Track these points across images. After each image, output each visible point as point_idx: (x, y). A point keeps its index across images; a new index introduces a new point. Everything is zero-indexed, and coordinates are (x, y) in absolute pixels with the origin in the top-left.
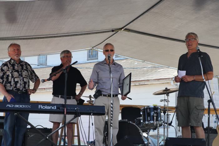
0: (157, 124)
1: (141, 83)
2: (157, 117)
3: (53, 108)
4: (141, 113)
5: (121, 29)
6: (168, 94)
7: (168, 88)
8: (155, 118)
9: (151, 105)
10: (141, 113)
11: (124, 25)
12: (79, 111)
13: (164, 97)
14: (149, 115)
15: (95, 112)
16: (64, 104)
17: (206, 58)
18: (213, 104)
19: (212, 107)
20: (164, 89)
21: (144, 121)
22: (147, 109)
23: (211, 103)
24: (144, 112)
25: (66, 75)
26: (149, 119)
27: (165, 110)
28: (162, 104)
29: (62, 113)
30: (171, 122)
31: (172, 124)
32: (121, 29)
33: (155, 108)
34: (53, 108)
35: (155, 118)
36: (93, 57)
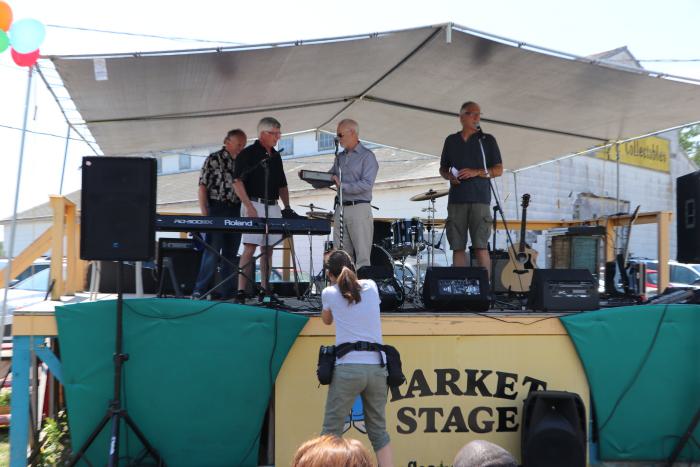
0: (416, 247)
1: (403, 184)
2: (417, 236)
3: (247, 224)
4: (392, 231)
5: (359, 96)
6: (433, 200)
7: (434, 190)
8: (413, 237)
9: (408, 218)
10: (392, 231)
11: (363, 91)
12: (289, 229)
13: (427, 203)
14: (404, 232)
15: (315, 229)
16: (264, 216)
17: (490, 141)
18: (501, 213)
19: (499, 218)
20: (428, 191)
21: (396, 242)
22: (400, 223)
23: (498, 212)
24: (396, 229)
25: (267, 171)
26: (404, 239)
27: (429, 225)
28: (423, 216)
29: (262, 231)
30: (439, 243)
31: (441, 247)
32: (359, 96)
33: (414, 222)
34: (247, 224)
35: (413, 237)
36: (327, 145)
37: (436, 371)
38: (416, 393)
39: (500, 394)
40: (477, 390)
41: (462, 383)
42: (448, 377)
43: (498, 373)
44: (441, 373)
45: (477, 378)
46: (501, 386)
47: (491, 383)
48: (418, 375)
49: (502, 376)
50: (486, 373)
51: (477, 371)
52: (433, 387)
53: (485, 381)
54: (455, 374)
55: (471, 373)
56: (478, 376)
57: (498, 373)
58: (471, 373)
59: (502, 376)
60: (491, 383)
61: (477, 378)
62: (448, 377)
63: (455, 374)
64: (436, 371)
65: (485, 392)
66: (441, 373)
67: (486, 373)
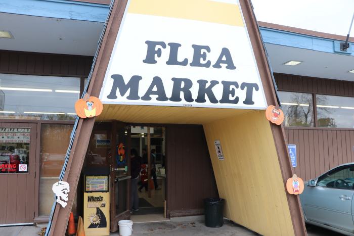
37: (173, 79)
38: (154, 97)
39: (225, 100)
40: (206, 98)
41: (195, 91)
42: (183, 85)
43: (223, 82)
44: (177, 82)
45: (206, 87)
46: (227, 92)
47: (218, 92)
48: (157, 81)
49: (226, 84)
50: (214, 83)
51: (207, 82)
52: (169, 94)
53: (214, 90)
54: (189, 83)
55: (202, 83)
56: (207, 85)
57: (223, 82)
58: (202, 83)
59: (226, 84)
60: (218, 92)
61: (206, 87)
62: (183, 85)
63: (189, 83)
64: (173, 79)
65: (213, 100)
66: (177, 82)
67: (214, 83)
